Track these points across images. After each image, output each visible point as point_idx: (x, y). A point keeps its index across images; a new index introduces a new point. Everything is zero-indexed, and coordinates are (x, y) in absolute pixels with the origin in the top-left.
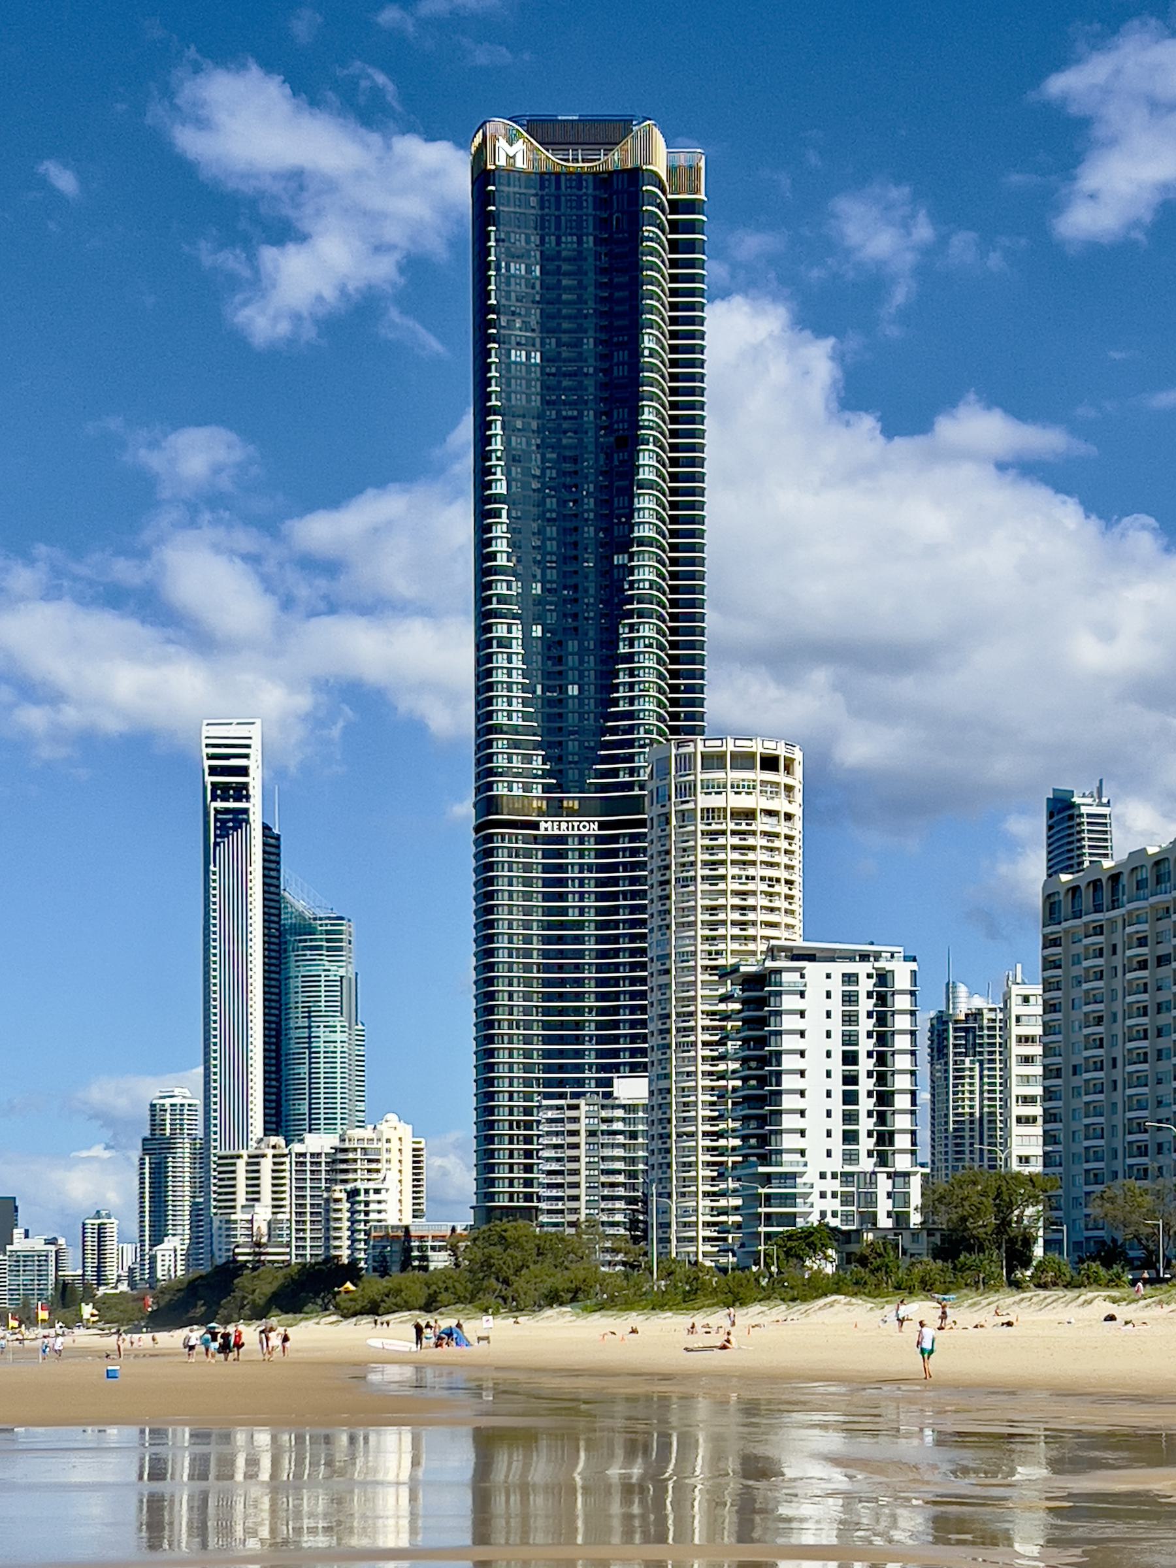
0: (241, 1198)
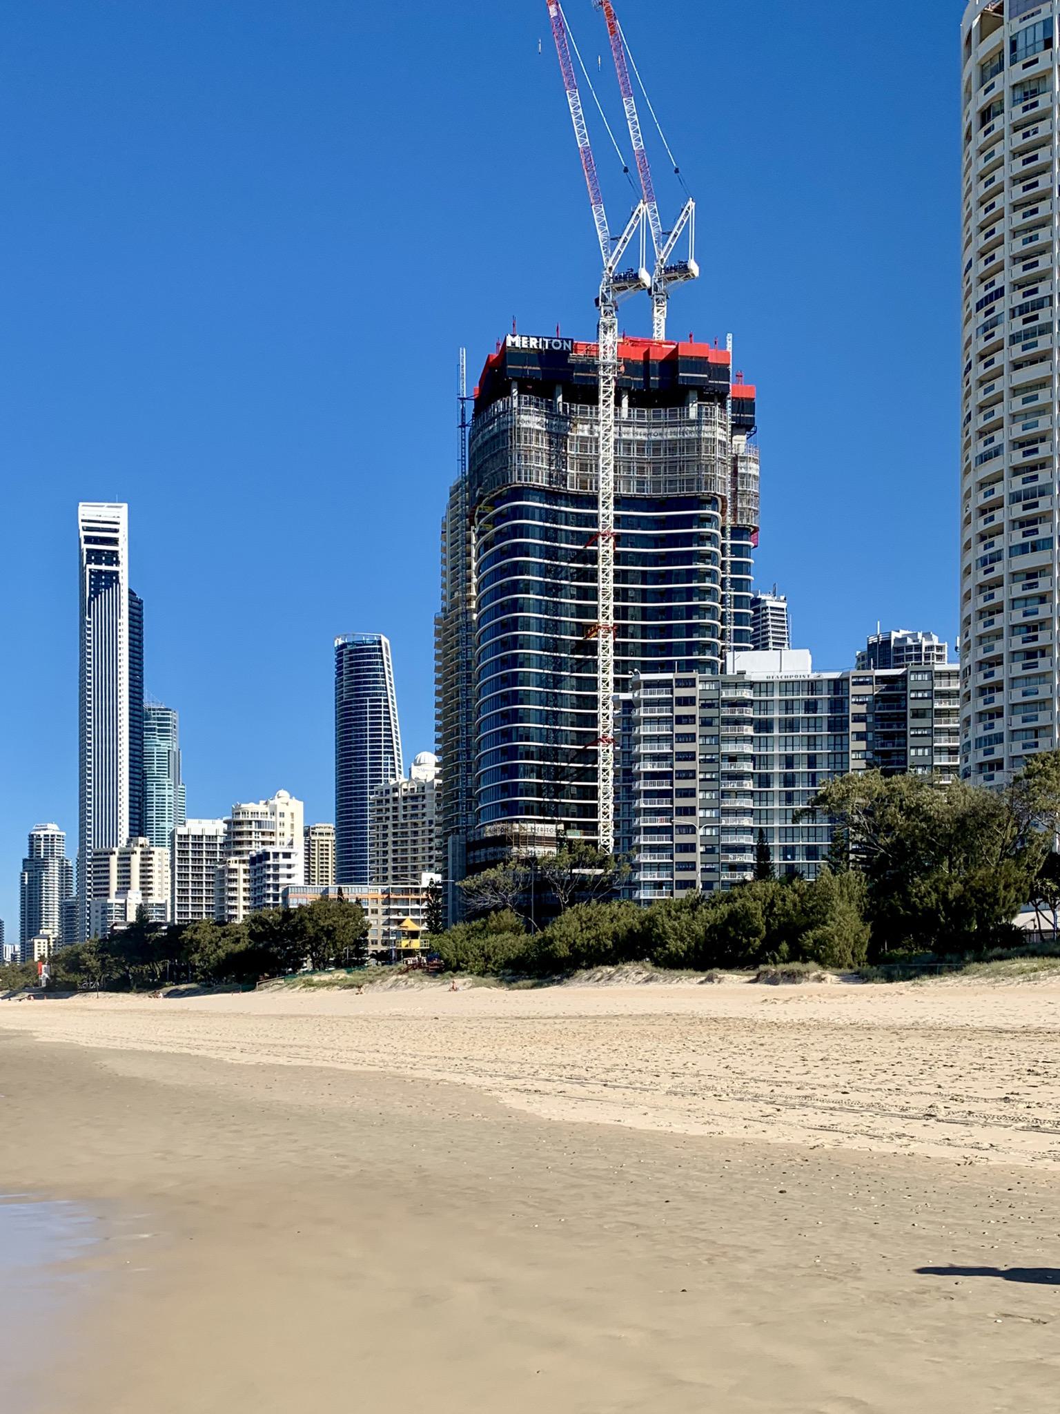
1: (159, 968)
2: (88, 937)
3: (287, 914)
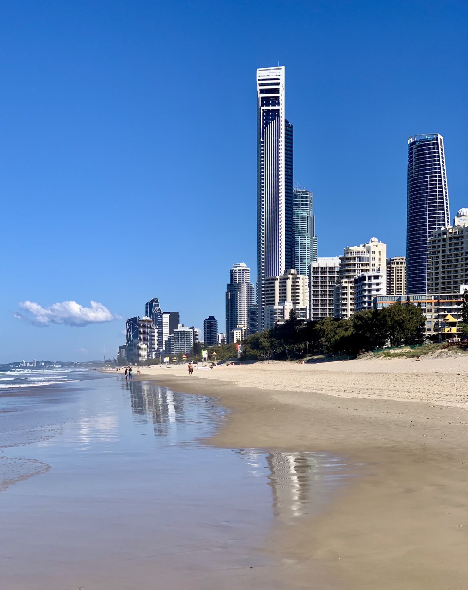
0: (277, 299)
1: (302, 346)
2: (263, 329)
3: (376, 313)
